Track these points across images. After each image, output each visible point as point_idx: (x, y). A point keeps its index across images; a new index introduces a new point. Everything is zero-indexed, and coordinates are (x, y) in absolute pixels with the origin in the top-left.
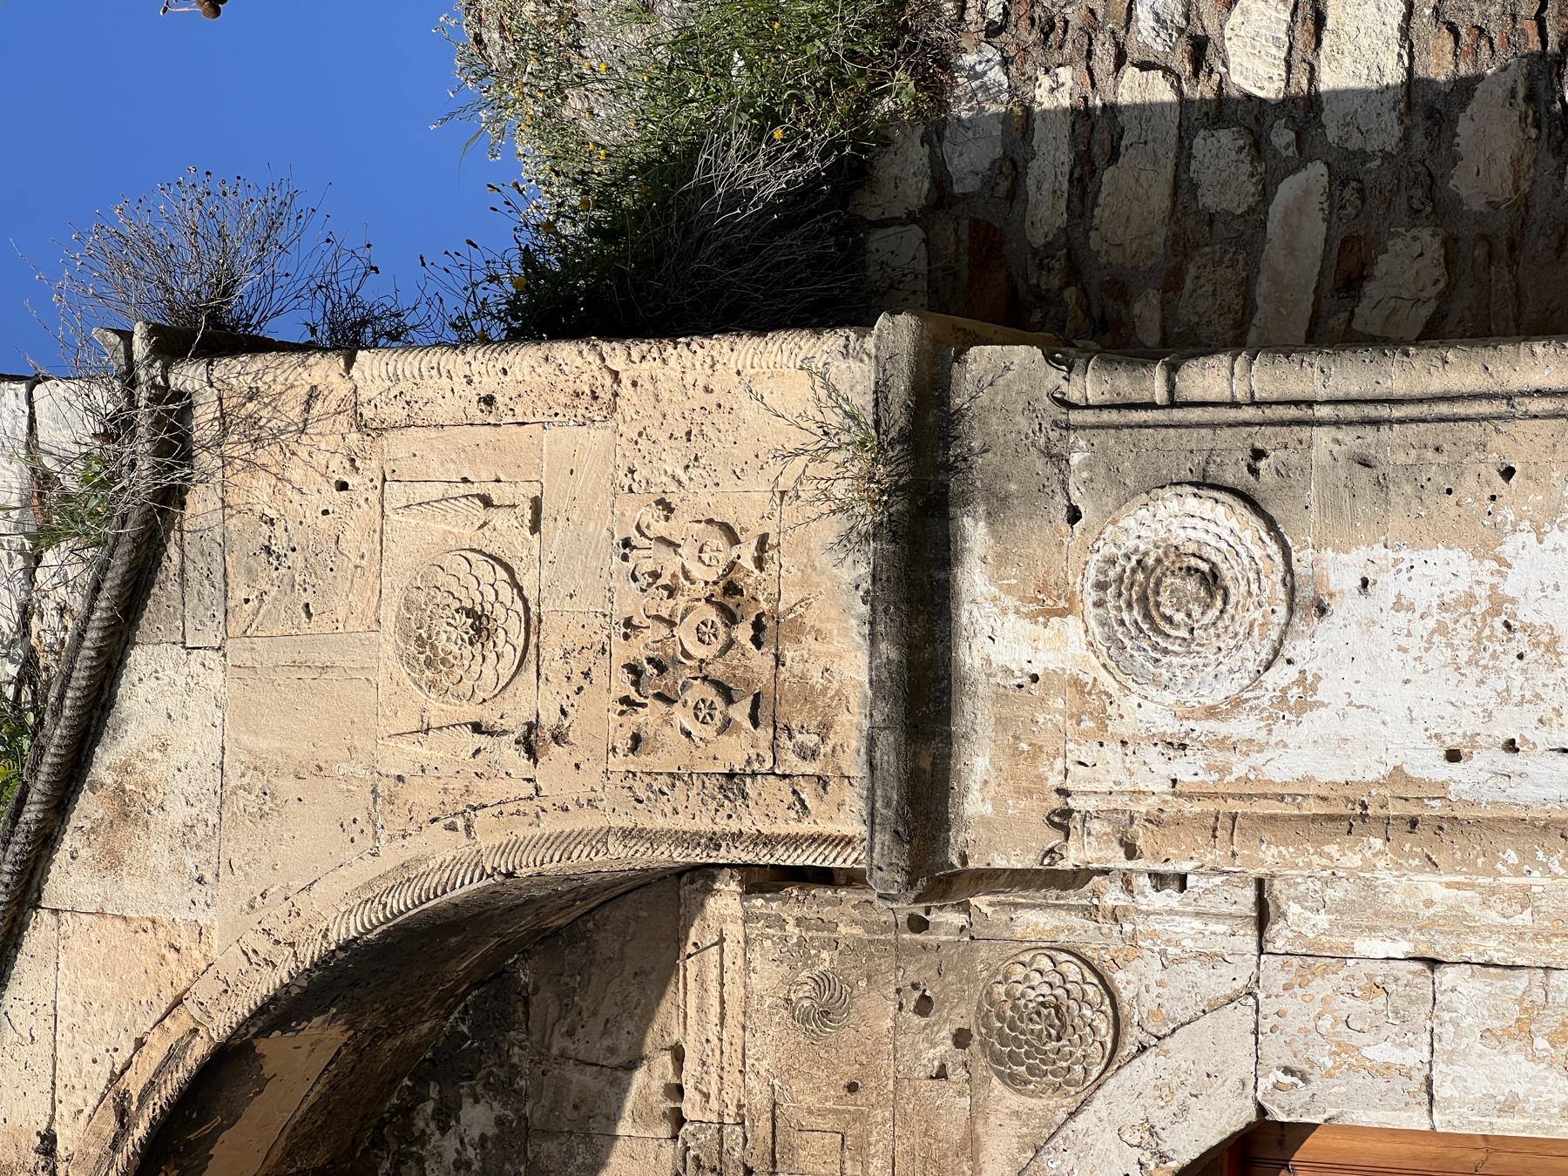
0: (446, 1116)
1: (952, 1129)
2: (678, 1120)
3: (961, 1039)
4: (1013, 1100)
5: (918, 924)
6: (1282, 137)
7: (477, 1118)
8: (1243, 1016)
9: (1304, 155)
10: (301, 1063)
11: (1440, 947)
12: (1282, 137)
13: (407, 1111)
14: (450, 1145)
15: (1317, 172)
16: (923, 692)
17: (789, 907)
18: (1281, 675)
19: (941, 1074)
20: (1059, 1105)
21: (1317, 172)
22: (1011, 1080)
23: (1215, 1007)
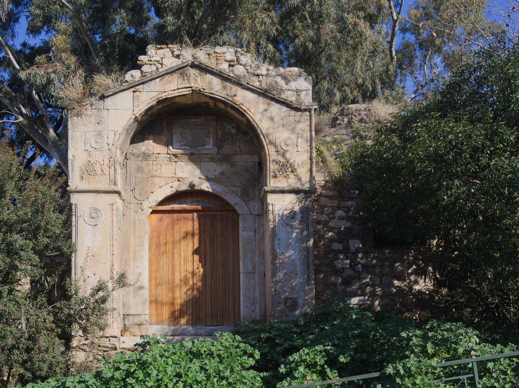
0: (233, 127)
1: (237, 184)
2: (234, 154)
3: (245, 185)
4: (239, 190)
5: (256, 180)
6: (331, 216)
7: (233, 131)
8: (249, 213)
9: (330, 218)
10: (241, 118)
11: (257, 231)
12: (331, 216)
13: (233, 123)
14: (230, 128)
15: (328, 219)
16: (282, 192)
17: (257, 167)
18: (285, 224)
19: (241, 183)
20: (239, 195)
21: (328, 219)
22: (241, 190)
23: (250, 210)
